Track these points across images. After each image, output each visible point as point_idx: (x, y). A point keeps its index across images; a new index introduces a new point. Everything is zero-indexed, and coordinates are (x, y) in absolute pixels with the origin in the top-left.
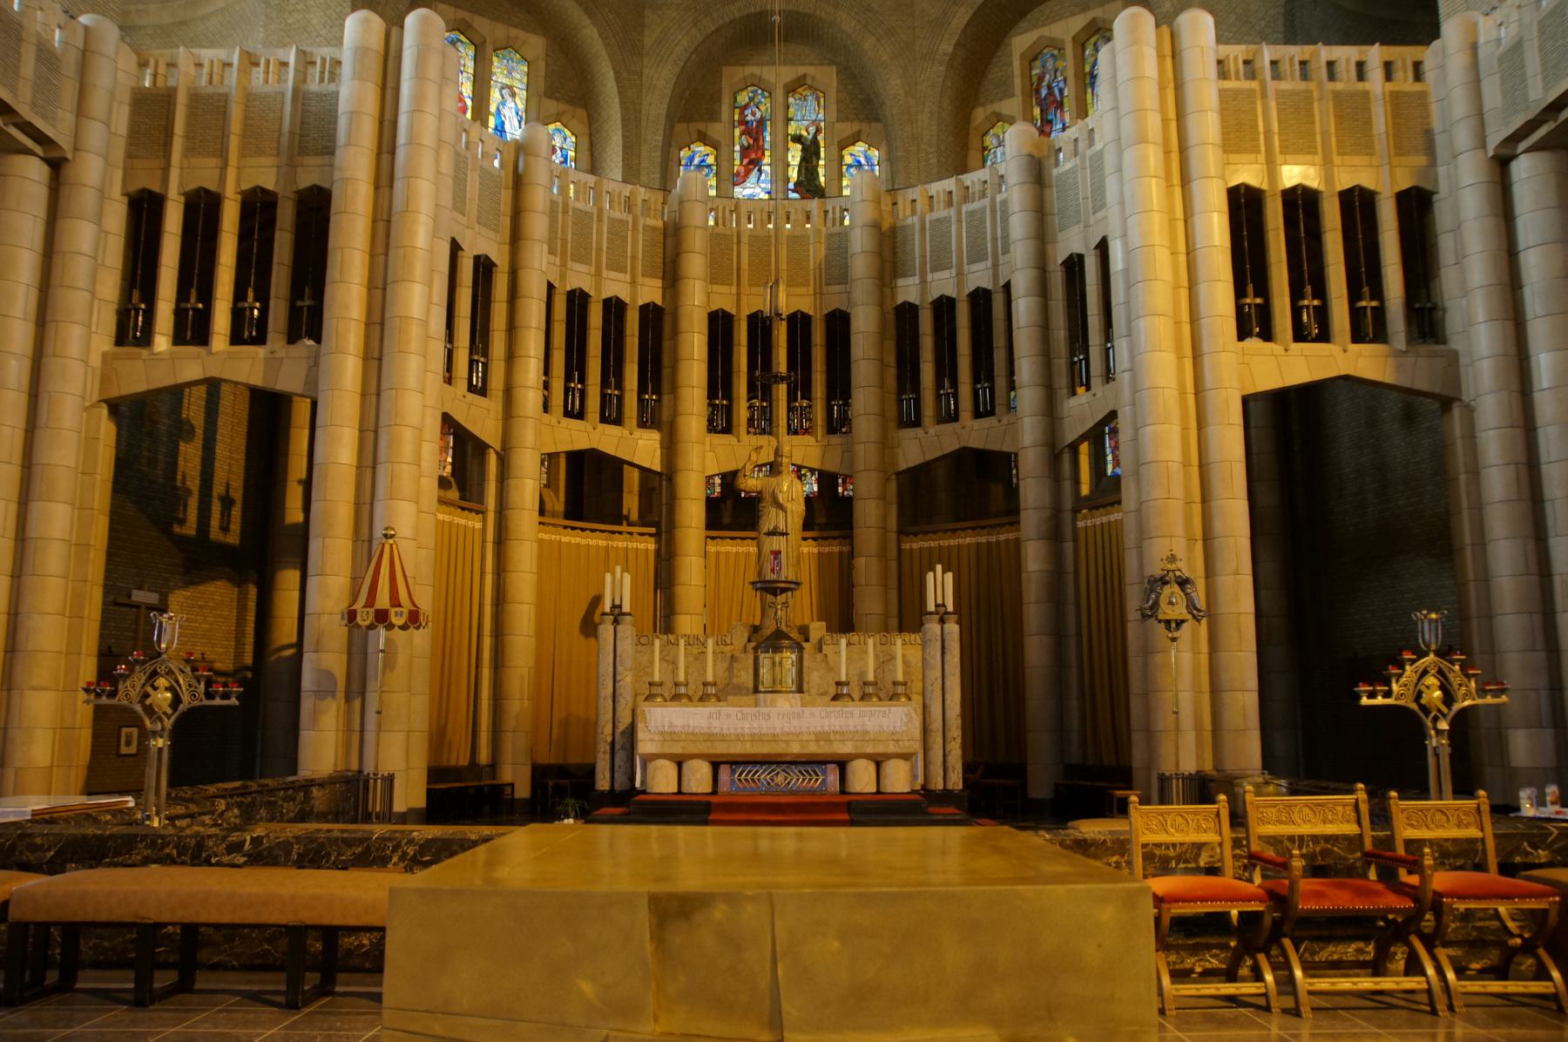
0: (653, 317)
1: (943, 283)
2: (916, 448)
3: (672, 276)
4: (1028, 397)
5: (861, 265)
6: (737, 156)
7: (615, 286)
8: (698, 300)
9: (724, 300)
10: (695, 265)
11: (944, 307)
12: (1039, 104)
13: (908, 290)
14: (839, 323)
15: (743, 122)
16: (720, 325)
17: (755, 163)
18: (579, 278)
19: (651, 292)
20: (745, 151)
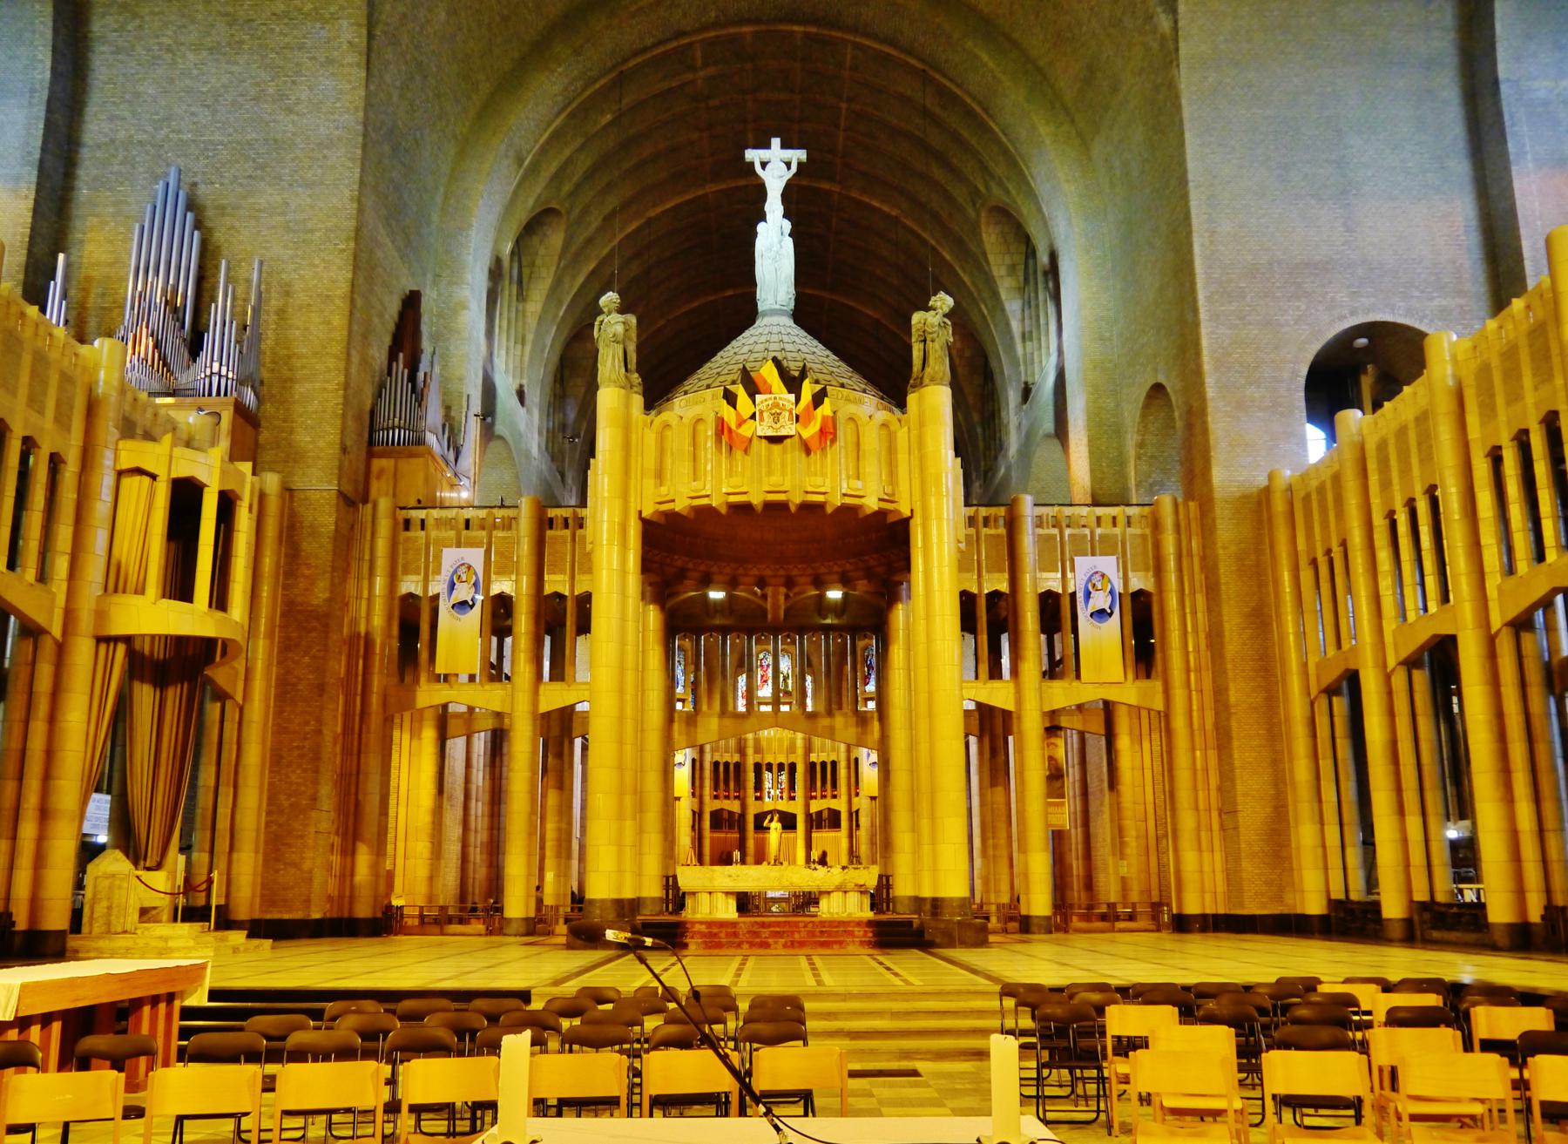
0: (737, 765)
1: (824, 757)
2: (815, 806)
3: (741, 750)
4: (844, 798)
5: (800, 751)
6: (759, 679)
7: (727, 758)
8: (751, 761)
9: (758, 759)
10: (750, 751)
11: (823, 764)
12: (868, 666)
13: (813, 758)
14: (793, 767)
15: (762, 666)
16: (758, 767)
17: (766, 681)
18: (717, 758)
19: (736, 758)
20: (762, 676)
